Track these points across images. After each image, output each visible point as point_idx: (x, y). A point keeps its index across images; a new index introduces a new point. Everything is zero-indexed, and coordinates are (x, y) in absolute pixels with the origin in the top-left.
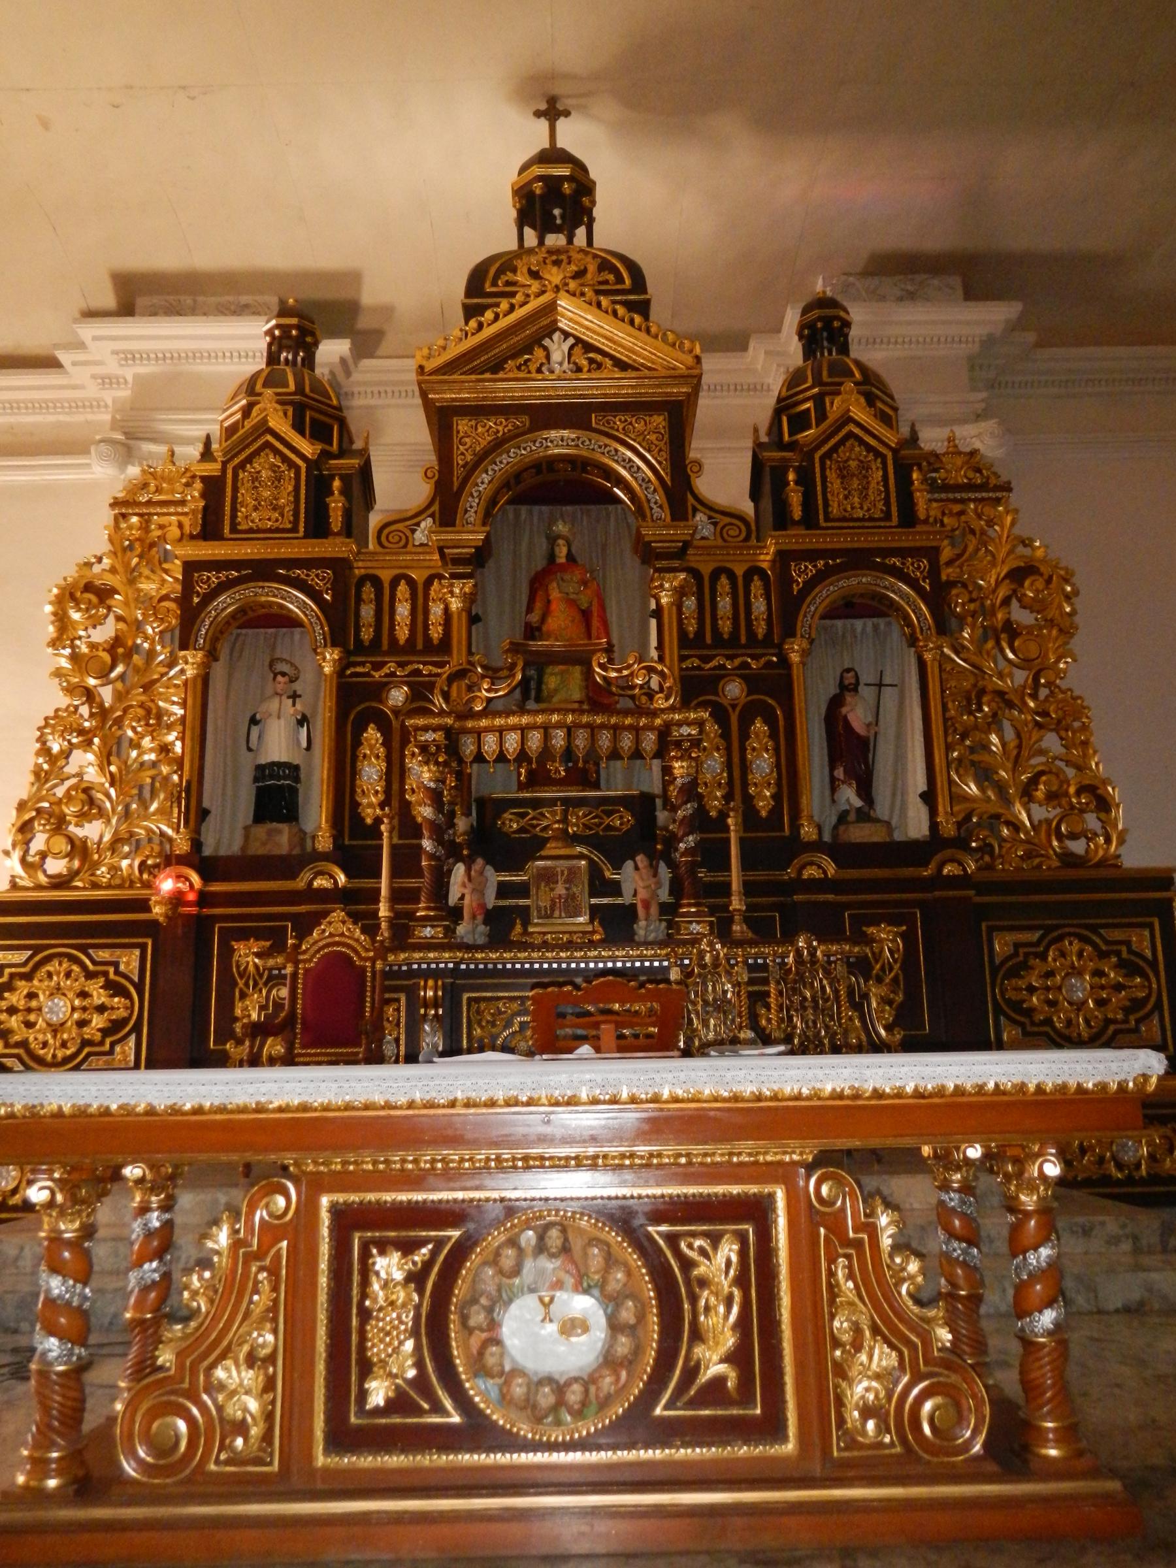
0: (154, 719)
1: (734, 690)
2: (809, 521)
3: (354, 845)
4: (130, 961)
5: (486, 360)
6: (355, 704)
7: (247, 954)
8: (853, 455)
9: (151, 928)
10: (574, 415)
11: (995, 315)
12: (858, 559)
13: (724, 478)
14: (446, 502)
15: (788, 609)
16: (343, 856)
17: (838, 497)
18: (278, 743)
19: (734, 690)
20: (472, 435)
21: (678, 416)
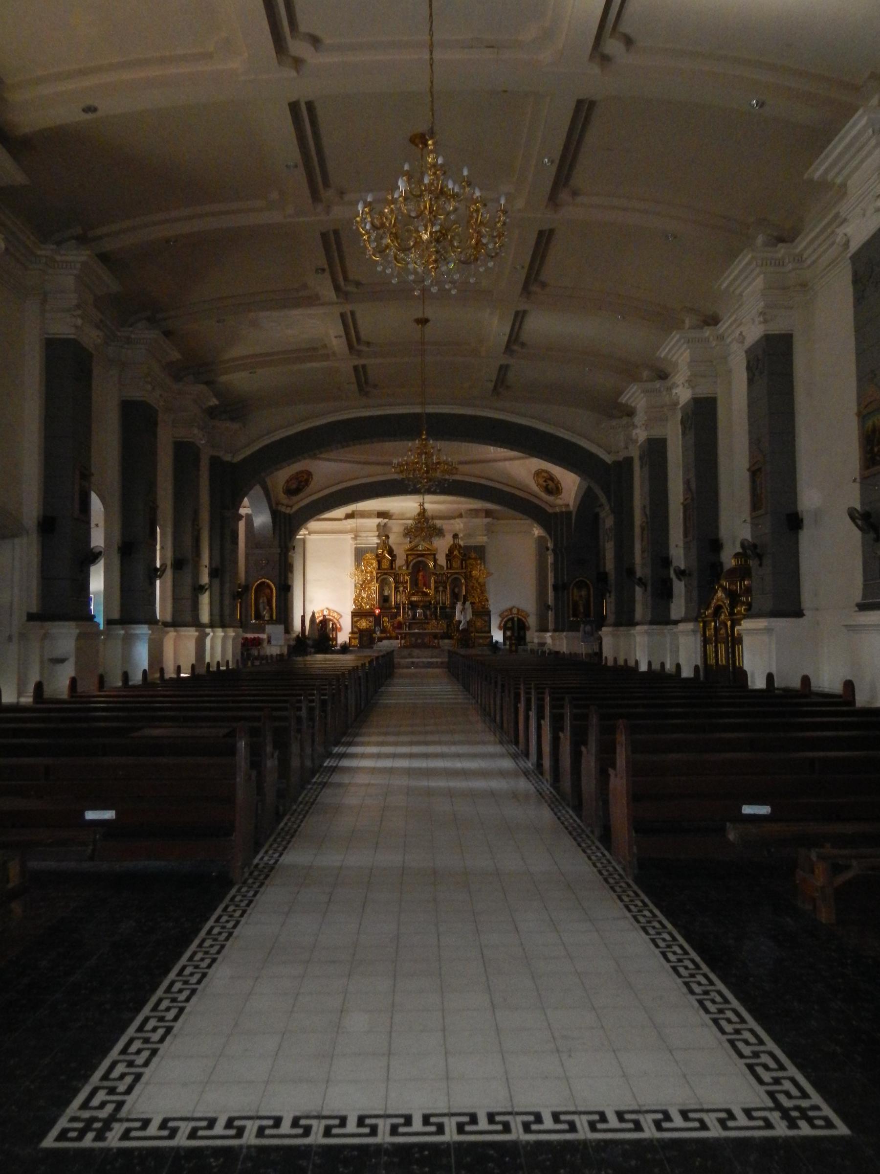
0: (369, 588)
1: (441, 589)
2: (451, 569)
3: (397, 607)
4: (371, 619)
5: (411, 549)
6: (396, 588)
7: (386, 619)
8: (456, 559)
9: (375, 616)
10: (422, 555)
11: (488, 520)
12: (456, 573)
13: (442, 560)
14: (408, 563)
15: (448, 578)
16: (396, 608)
17: (454, 565)
18: (386, 593)
19: (441, 589)
20: (410, 558)
21: (435, 555)
